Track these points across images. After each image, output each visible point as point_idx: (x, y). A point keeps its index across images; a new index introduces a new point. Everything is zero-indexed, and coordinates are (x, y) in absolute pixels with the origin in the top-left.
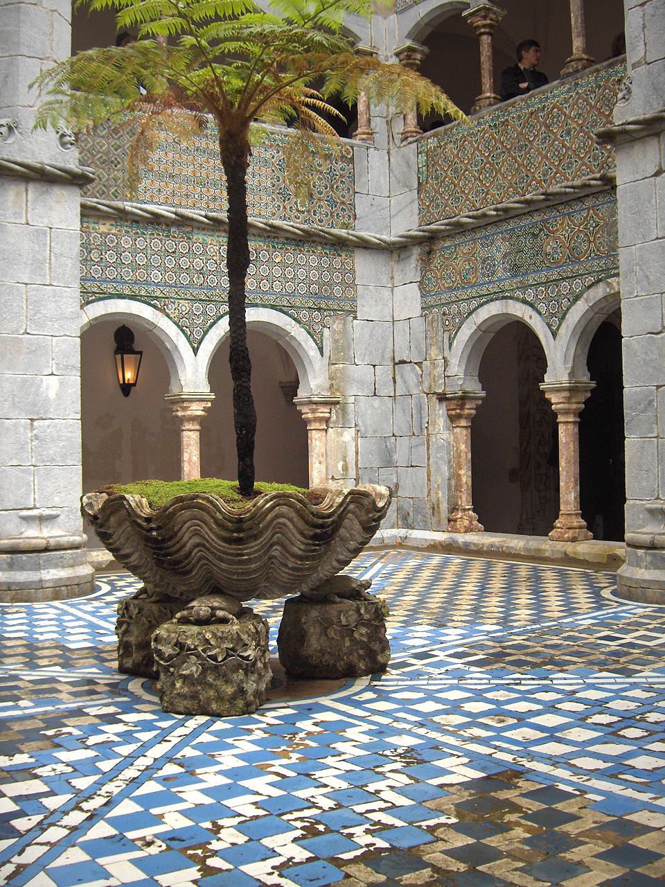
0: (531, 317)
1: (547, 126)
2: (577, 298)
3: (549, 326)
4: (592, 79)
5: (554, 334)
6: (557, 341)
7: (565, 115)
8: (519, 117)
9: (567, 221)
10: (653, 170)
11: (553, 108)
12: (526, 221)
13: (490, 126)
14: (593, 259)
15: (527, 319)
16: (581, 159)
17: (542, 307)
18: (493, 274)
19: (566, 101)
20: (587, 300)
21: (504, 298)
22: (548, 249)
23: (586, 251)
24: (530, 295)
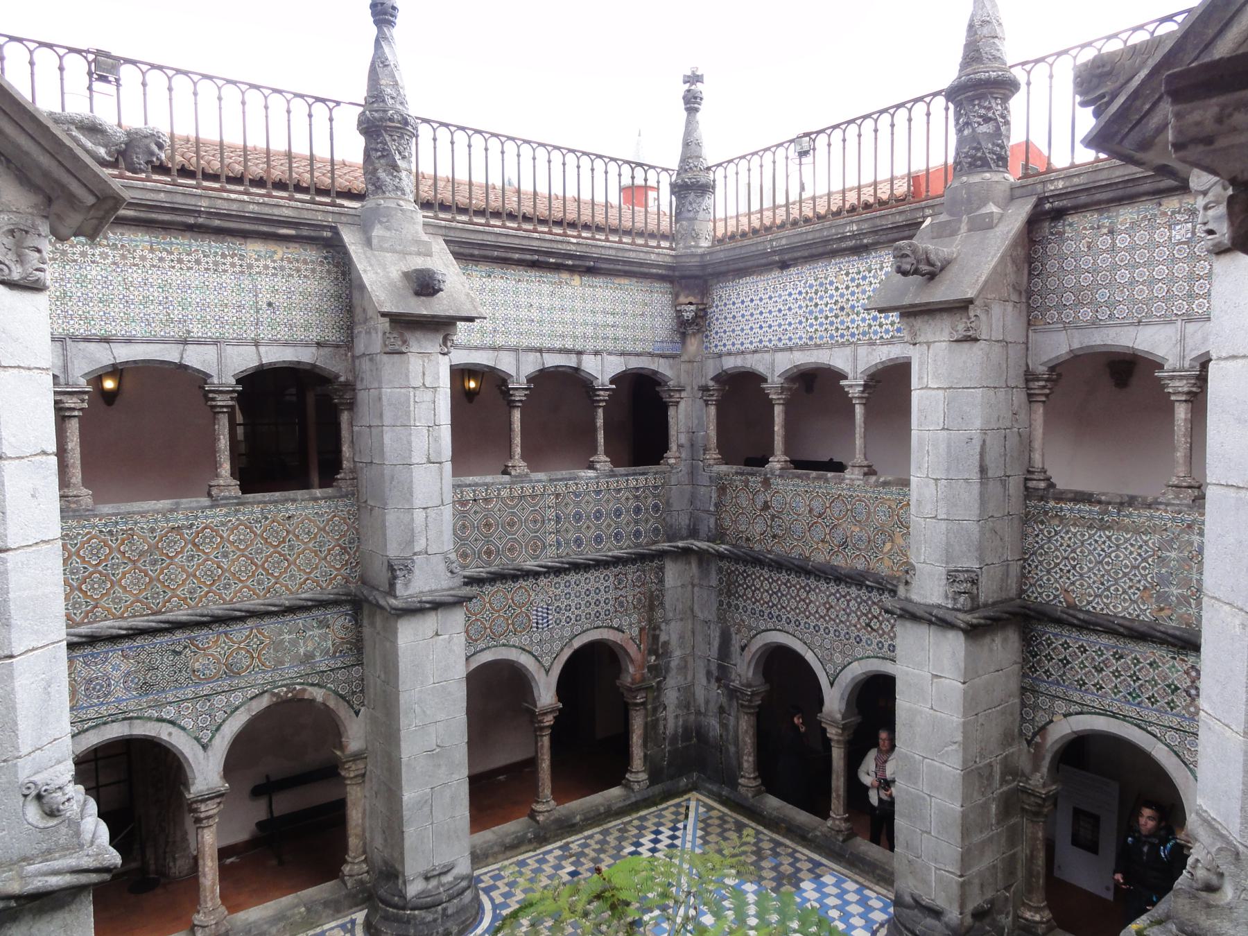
0: (170, 734)
1: (195, 545)
2: (237, 708)
3: (197, 739)
4: (257, 509)
5: (205, 747)
6: (210, 752)
7: (222, 537)
8: (152, 530)
9: (223, 637)
10: (431, 634)
11: (205, 528)
12: (166, 638)
13: (101, 532)
14: (257, 673)
15: (165, 737)
16: (241, 581)
17: (188, 723)
18: (106, 696)
19: (223, 524)
20: (249, 710)
21: (124, 719)
22: (197, 666)
23: (248, 667)
24: (170, 712)
